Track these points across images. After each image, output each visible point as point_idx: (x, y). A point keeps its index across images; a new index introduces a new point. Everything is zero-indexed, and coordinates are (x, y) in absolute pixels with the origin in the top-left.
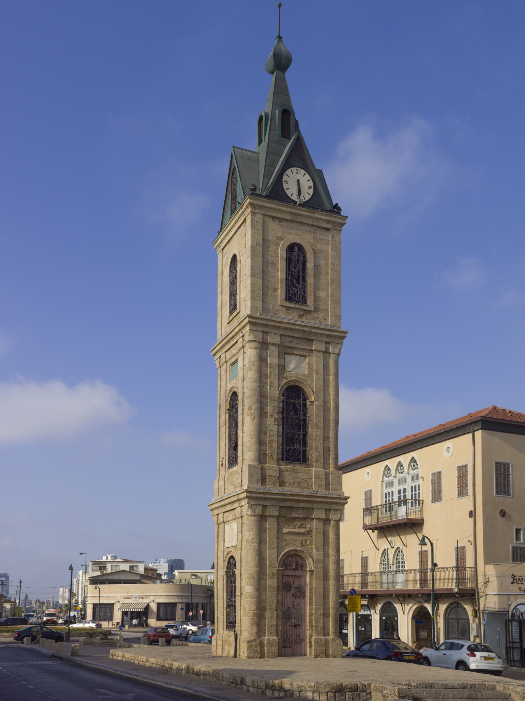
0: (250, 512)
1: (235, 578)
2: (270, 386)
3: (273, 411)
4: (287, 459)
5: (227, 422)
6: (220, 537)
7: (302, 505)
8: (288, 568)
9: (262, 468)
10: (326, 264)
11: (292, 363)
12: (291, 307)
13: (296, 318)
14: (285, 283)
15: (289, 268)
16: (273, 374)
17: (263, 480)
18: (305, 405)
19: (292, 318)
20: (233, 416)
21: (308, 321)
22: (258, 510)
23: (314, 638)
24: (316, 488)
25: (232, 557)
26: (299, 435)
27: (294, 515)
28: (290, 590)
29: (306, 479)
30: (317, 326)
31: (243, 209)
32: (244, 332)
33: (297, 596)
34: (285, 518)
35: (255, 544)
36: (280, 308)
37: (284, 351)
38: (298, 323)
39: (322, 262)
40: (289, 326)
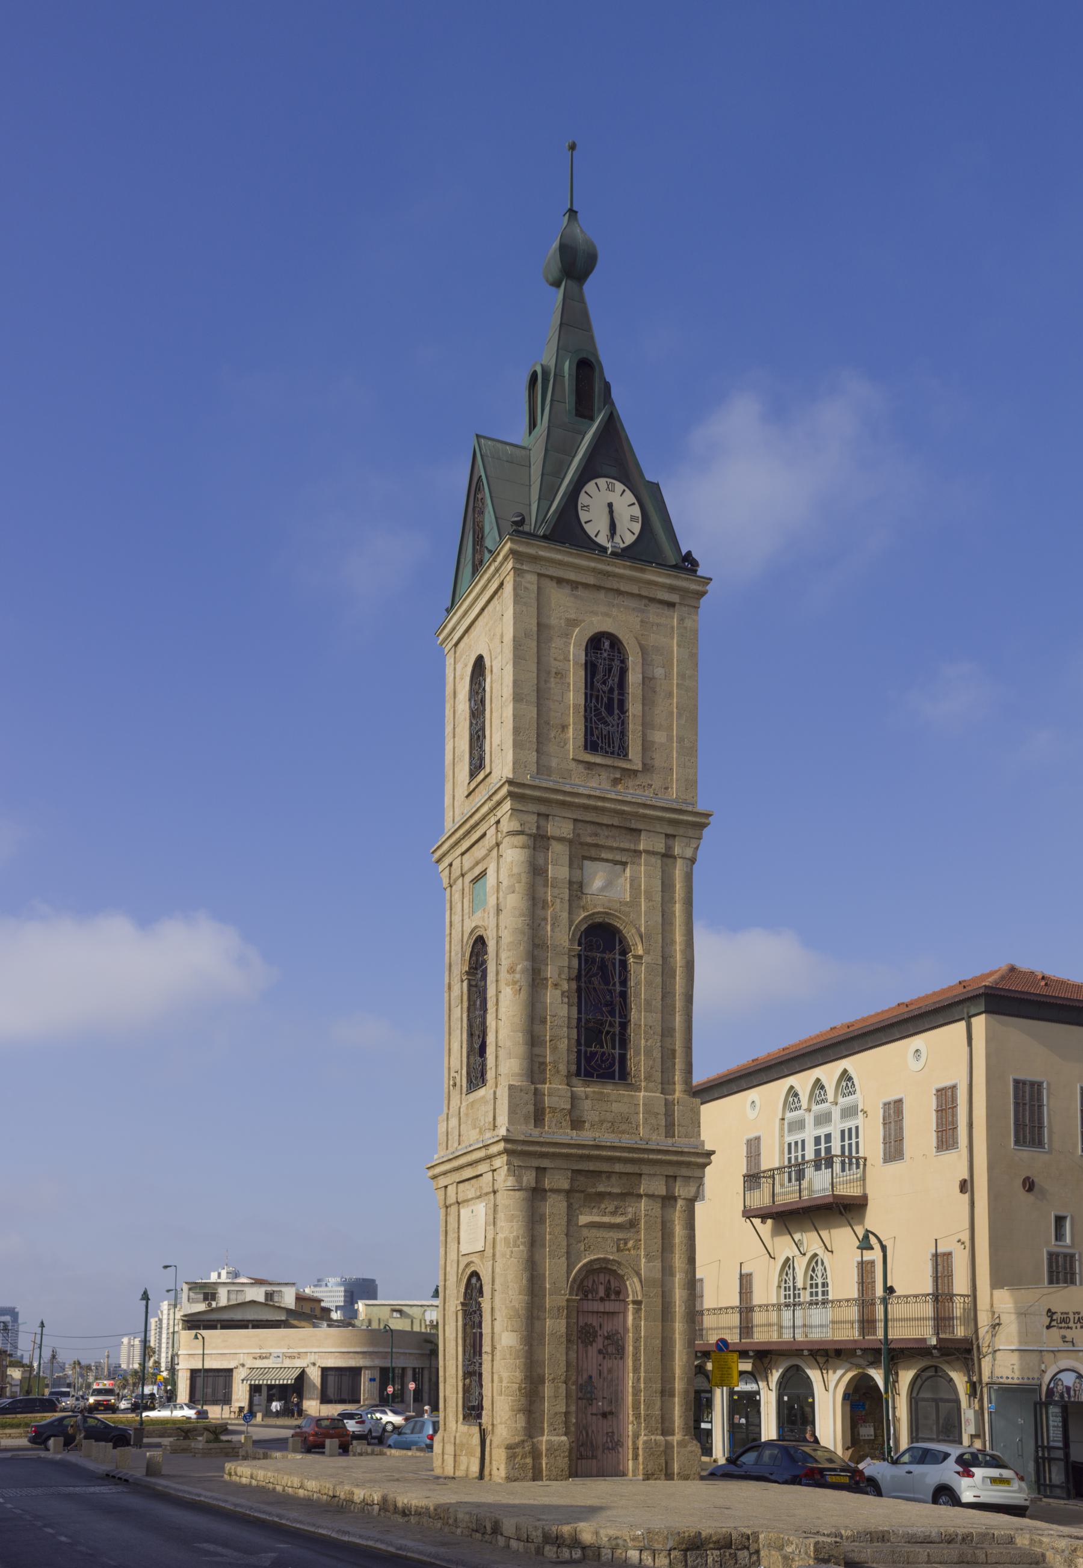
0: (511, 1182)
1: (481, 1316)
2: (553, 925)
3: (559, 975)
4: (588, 1074)
5: (465, 998)
6: (450, 1232)
7: (618, 1167)
8: (590, 1296)
9: (536, 1092)
10: (668, 676)
11: (597, 878)
12: (595, 764)
13: (606, 785)
14: (582, 713)
15: (592, 683)
16: (558, 901)
17: (538, 1118)
18: (624, 964)
19: (596, 785)
20: (476, 986)
21: (631, 792)
22: (529, 1178)
23: (642, 1438)
24: (646, 1134)
25: (475, 1274)
26: (611, 1025)
27: (601, 1188)
28: (594, 1341)
29: (625, 1114)
30: (649, 802)
31: (496, 564)
32: (499, 814)
33: (607, 1353)
35: (522, 1248)
36: (573, 765)
37: (582, 853)
38: (609, 796)
39: (659, 672)
40: (592, 802)
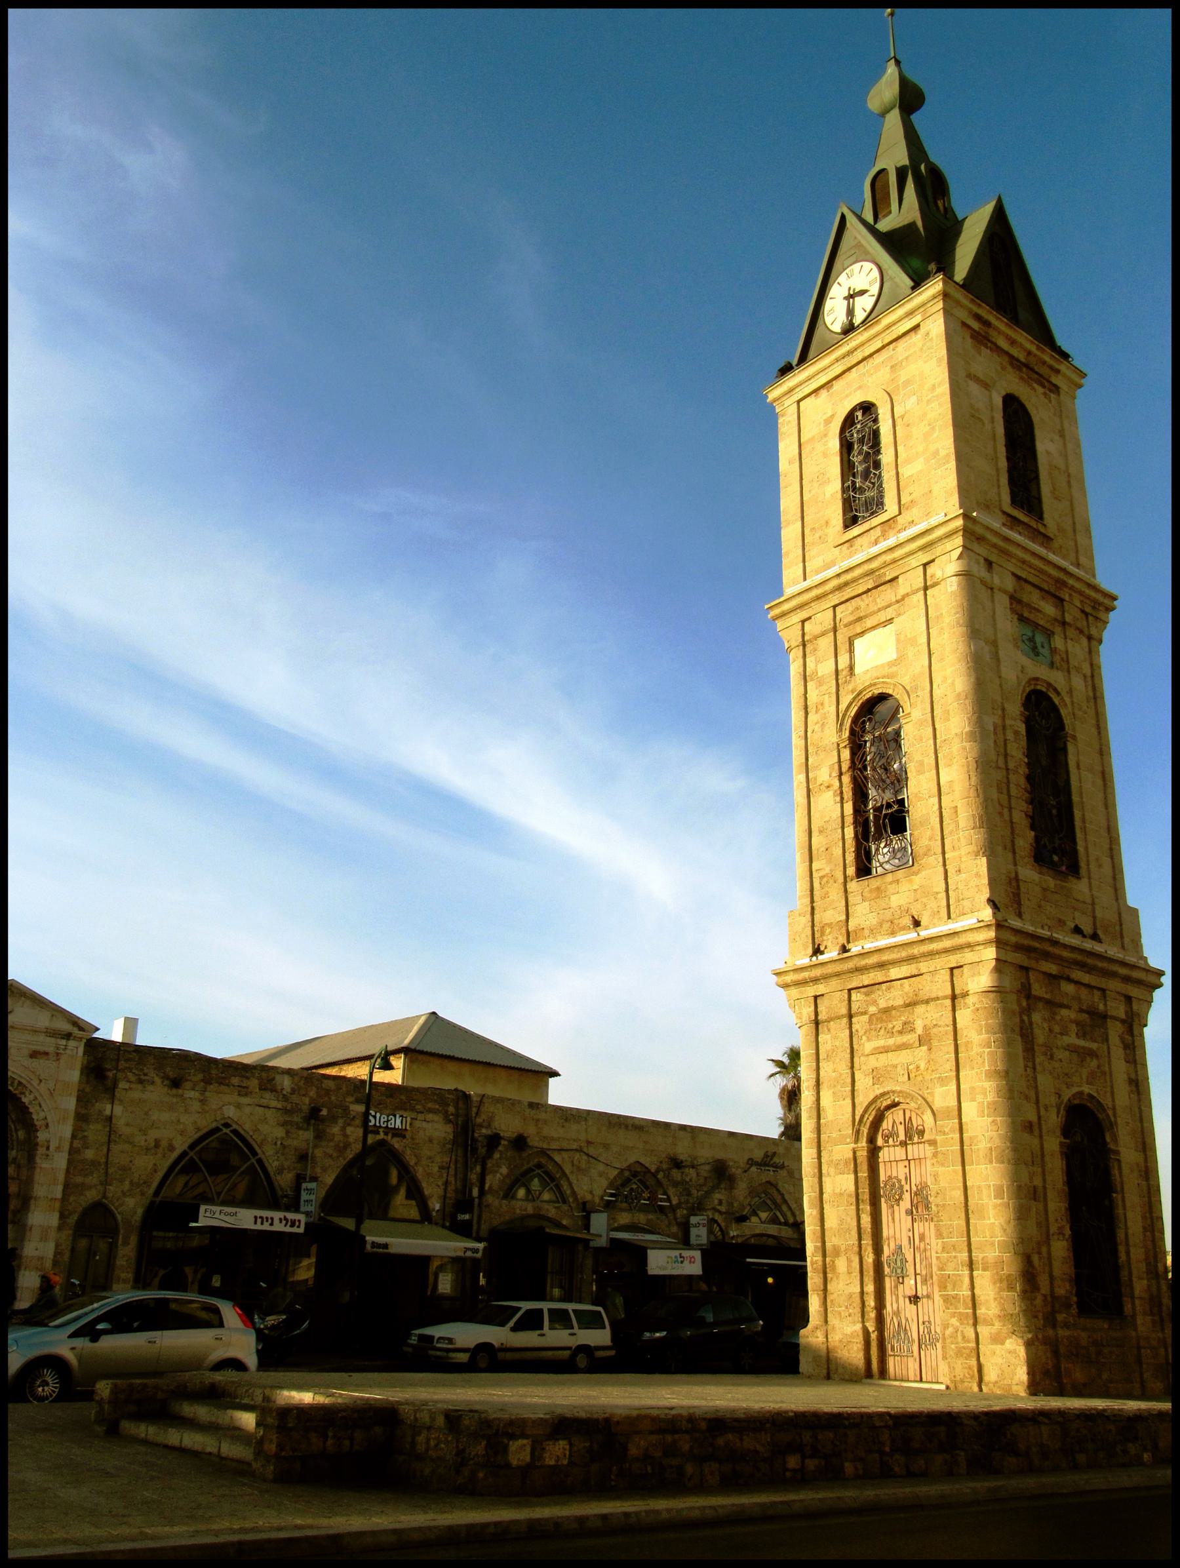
7: (895, 973)
27: (882, 1004)
28: (901, 1198)
34: (866, 1018)
